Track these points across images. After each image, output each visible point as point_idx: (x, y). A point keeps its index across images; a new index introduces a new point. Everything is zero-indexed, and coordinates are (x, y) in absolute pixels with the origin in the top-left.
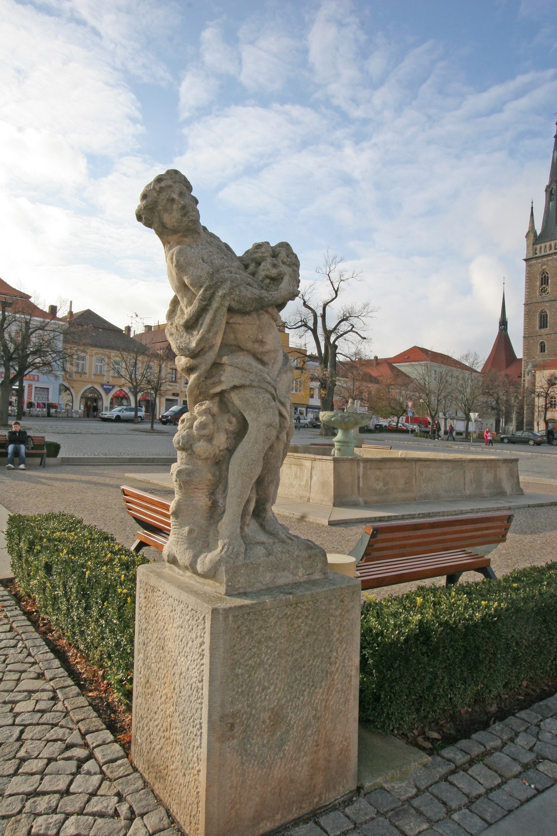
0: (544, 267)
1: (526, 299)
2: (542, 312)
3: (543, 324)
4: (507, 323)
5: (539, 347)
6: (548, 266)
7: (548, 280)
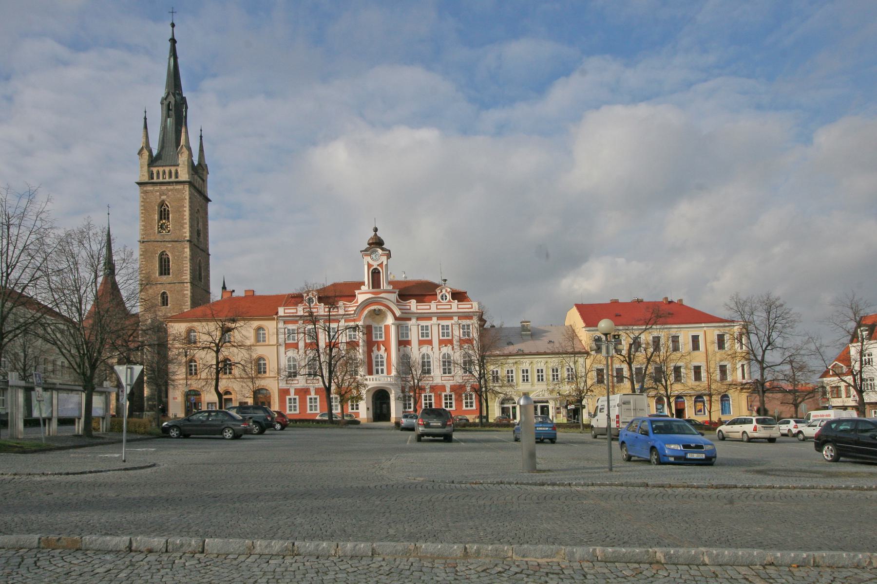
0: (162, 197)
2: (162, 254)
6: (168, 197)
7: (168, 214)
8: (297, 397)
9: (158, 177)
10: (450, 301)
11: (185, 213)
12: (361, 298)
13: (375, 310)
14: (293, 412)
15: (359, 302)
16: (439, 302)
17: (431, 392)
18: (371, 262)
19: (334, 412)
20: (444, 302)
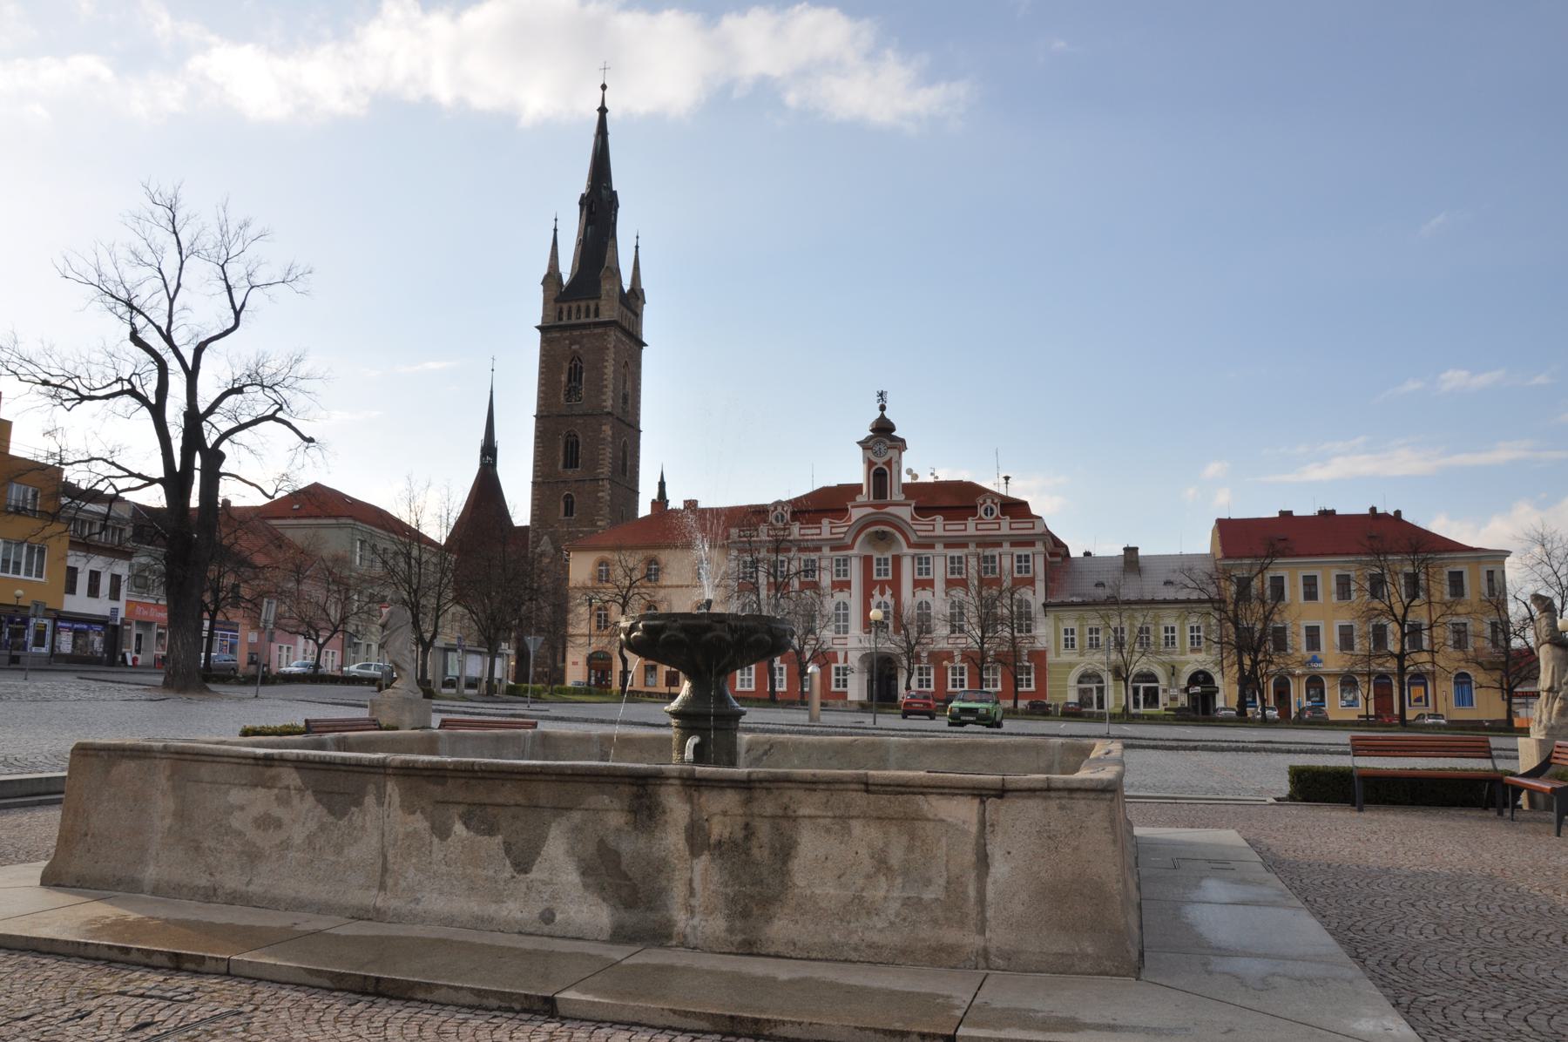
0: (573, 347)
1: (539, 406)
3: (572, 460)
4: (495, 450)
5: (562, 505)
8: (965, 665)
9: (569, 317)
10: (997, 518)
11: (606, 371)
12: (856, 514)
13: (877, 532)
14: (746, 689)
15: (853, 519)
16: (981, 518)
17: (962, 661)
18: (874, 459)
19: (777, 689)
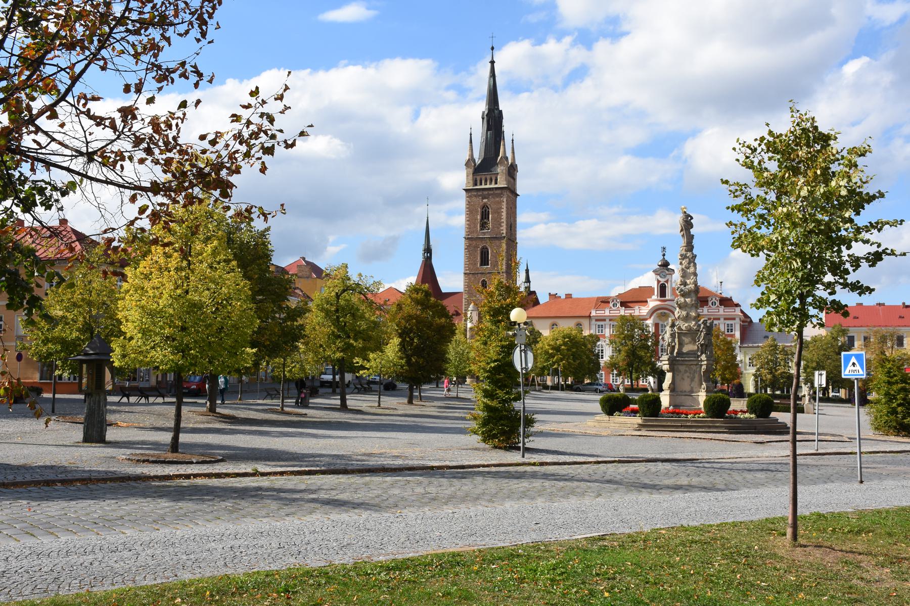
3: (484, 261)
20: (714, 307)
